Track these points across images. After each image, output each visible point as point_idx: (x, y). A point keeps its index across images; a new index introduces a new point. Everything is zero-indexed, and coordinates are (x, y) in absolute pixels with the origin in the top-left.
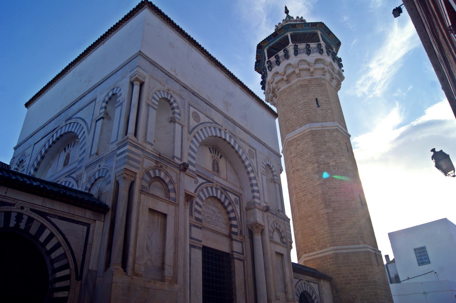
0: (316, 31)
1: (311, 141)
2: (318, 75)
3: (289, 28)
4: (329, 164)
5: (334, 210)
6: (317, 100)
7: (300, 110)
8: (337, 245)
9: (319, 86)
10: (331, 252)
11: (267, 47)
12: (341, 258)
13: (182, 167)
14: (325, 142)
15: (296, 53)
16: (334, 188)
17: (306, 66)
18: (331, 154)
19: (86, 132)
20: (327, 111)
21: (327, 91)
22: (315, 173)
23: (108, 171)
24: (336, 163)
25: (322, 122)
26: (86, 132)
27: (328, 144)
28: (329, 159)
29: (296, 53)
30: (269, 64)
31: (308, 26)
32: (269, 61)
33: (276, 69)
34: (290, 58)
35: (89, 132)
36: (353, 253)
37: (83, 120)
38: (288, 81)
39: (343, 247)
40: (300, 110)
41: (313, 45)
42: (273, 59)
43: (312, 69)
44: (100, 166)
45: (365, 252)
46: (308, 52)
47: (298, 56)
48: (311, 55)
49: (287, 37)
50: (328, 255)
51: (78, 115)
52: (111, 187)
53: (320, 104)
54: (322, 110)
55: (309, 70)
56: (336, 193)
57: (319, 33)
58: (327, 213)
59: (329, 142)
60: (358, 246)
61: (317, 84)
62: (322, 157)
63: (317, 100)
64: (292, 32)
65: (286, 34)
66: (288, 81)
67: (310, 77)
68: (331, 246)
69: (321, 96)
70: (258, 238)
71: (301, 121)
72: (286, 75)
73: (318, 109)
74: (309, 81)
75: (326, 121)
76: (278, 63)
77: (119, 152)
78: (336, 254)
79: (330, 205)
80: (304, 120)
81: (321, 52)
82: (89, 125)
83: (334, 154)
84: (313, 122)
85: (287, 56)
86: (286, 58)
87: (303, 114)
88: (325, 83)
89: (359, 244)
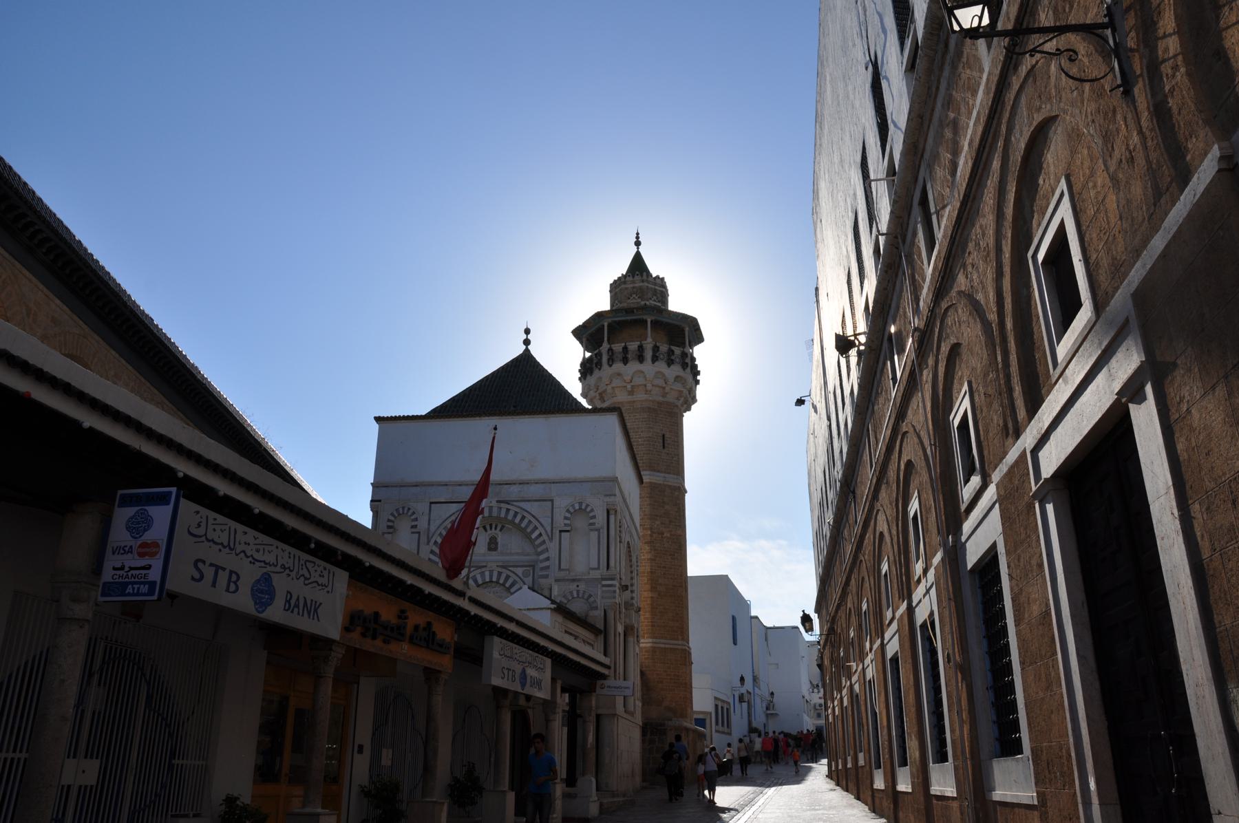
2: (671, 398)
15: (655, 359)
17: (660, 382)
19: (545, 537)
23: (590, 596)
26: (545, 537)
27: (667, 507)
29: (655, 359)
32: (610, 350)
33: (618, 366)
35: (551, 539)
38: (631, 393)
41: (677, 351)
42: (618, 347)
43: (667, 389)
46: (670, 363)
52: (599, 613)
57: (687, 329)
66: (631, 393)
67: (661, 399)
70: (631, 639)
74: (660, 403)
81: (684, 366)
82: (549, 529)
85: (641, 359)
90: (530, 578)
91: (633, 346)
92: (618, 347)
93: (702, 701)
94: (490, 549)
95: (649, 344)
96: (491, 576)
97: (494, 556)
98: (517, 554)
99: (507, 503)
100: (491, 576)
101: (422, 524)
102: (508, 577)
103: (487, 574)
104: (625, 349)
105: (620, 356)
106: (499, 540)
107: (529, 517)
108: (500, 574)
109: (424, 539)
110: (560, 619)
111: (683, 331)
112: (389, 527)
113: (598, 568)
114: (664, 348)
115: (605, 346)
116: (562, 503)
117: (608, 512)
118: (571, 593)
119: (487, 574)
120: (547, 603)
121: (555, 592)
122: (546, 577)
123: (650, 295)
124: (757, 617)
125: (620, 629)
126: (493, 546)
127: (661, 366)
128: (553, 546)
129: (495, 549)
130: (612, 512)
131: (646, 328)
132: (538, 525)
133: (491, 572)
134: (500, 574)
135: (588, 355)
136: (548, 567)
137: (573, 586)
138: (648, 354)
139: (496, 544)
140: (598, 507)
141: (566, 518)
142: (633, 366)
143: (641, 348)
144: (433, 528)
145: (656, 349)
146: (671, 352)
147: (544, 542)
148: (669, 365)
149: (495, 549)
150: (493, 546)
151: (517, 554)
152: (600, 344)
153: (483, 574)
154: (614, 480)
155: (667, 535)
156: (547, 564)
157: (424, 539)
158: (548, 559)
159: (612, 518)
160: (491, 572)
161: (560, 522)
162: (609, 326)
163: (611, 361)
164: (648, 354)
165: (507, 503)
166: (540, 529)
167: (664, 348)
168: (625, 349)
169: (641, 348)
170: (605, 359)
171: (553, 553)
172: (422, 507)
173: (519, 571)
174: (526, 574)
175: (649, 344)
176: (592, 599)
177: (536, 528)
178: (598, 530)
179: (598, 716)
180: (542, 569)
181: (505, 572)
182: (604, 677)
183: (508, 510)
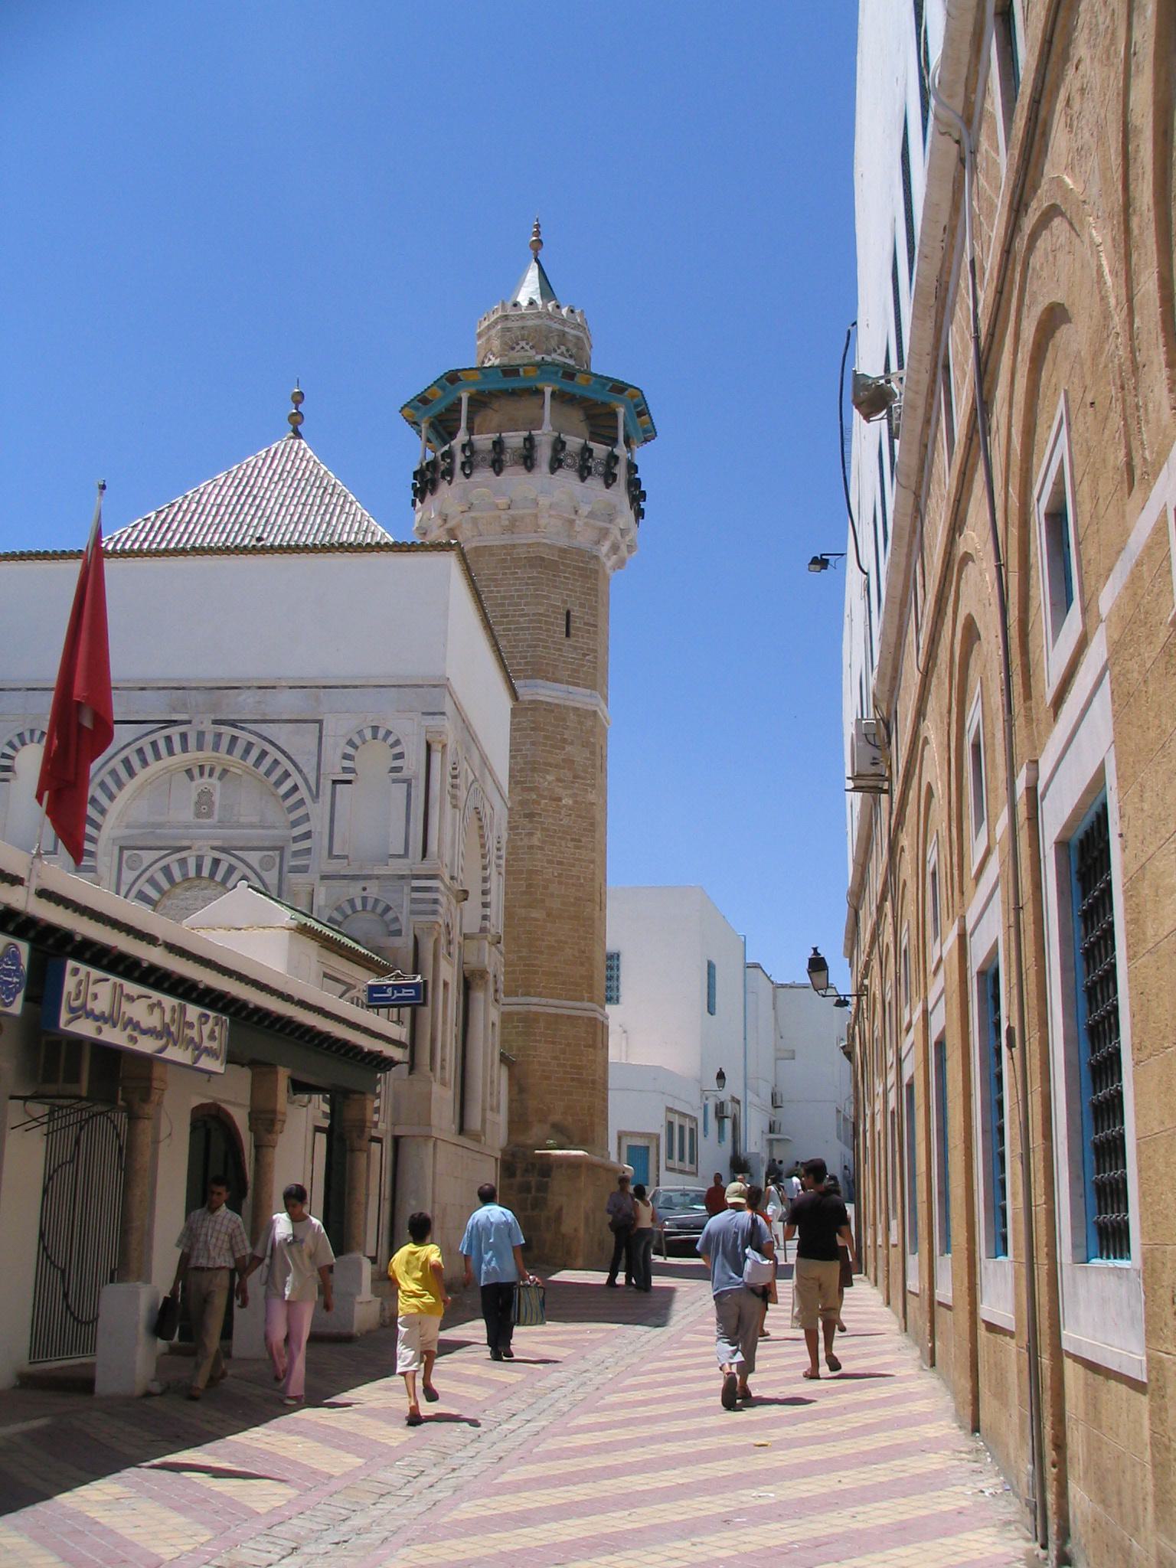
0: (615, 403)
1: (532, 729)
2: (583, 539)
3: (556, 373)
4: (560, 799)
5: (548, 915)
6: (568, 613)
7: (522, 629)
8: (540, 995)
9: (581, 575)
10: (526, 1008)
11: (473, 390)
12: (542, 1025)
13: (462, 896)
14: (564, 741)
15: (556, 464)
16: (560, 863)
18: (569, 775)
19: (303, 792)
20: (585, 655)
21: (596, 596)
22: (526, 816)
23: (388, 909)
24: (576, 802)
25: (568, 683)
26: (303, 792)
27: (568, 748)
28: (565, 788)
29: (556, 464)
30: (468, 454)
31: (604, 385)
34: (536, 470)
35: (316, 797)
36: (569, 1017)
37: (283, 752)
39: (551, 1001)
40: (522, 629)
41: (600, 450)
44: (364, 889)
45: (590, 1019)
47: (560, 472)
48: (589, 481)
49: (539, 393)
50: (518, 1013)
51: (266, 729)
52: (405, 943)
53: (572, 631)
54: (575, 648)
55: (572, 522)
56: (560, 875)
57: (621, 411)
58: (536, 920)
59: (572, 743)
60: (578, 1004)
61: (578, 568)
62: (550, 778)
63: (568, 613)
64: (557, 387)
65: (540, 385)
68: (528, 994)
69: (582, 605)
70: (478, 996)
71: (519, 664)
72: (511, 512)
73: (567, 642)
75: (577, 685)
76: (498, 466)
77: (416, 883)
78: (536, 1013)
79: (543, 901)
80: (526, 664)
83: (575, 777)
84: (548, 679)
86: (525, 463)
87: (529, 646)
88: (597, 572)
89: (581, 999)
90: (275, 871)
91: (514, 439)
92: (484, 441)
93: (630, 1114)
94: (198, 815)
95: (544, 437)
96: (199, 868)
98: (252, 826)
99: (233, 724)
100: (199, 868)
104: (498, 444)
105: (490, 457)
106: (217, 798)
107: (273, 753)
108: (216, 862)
110: (312, 947)
111: (614, 415)
113: (406, 855)
114: (574, 443)
115: (462, 437)
116: (338, 729)
117: (429, 746)
118: (351, 902)
120: (285, 916)
121: (320, 899)
122: (304, 869)
123: (554, 343)
124: (757, 966)
125: (449, 972)
127: (567, 478)
128: (318, 812)
130: (436, 747)
131: (542, 407)
132: (291, 769)
133: (200, 860)
134: (216, 862)
135: (430, 456)
136: (308, 851)
137: (354, 890)
138: (544, 454)
139: (211, 804)
140: (411, 734)
141: (346, 757)
142: (515, 479)
143: (530, 440)
145: (559, 445)
146: (587, 451)
147: (302, 802)
148: (583, 479)
149: (209, 815)
151: (252, 826)
152: (452, 435)
153: (183, 862)
154: (442, 685)
155: (567, 801)
156: (305, 844)
158: (308, 835)
159: (436, 758)
160: (200, 860)
161: (333, 766)
162: (470, 399)
163: (469, 466)
164: (544, 454)
165: (233, 724)
166: (296, 778)
167: (574, 443)
168: (498, 444)
169: (530, 440)
170: (459, 458)
171: (318, 824)
173: (253, 857)
174: (266, 864)
175: (544, 437)
176: (391, 915)
177: (287, 775)
178: (408, 782)
179: (397, 1140)
180: (296, 854)
181: (227, 861)
182: (384, 1063)
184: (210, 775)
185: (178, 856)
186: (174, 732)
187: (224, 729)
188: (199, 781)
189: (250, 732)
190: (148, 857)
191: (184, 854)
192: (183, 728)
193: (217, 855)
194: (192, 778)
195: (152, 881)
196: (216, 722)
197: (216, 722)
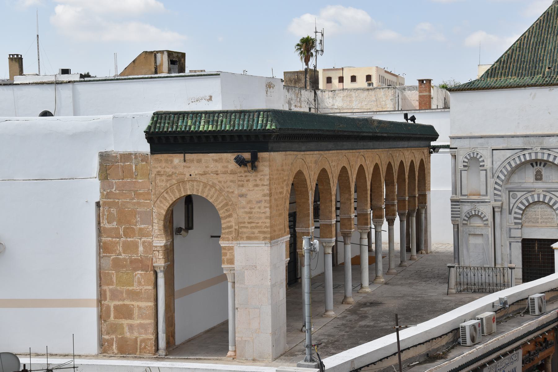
94: (537, 179)
96: (539, 197)
97: (539, 184)
99: (549, 149)
101: (488, 164)
102: (551, 199)
103: (536, 196)
106: (543, 173)
109: (489, 174)
112: (465, 166)
119: (536, 196)
126: (539, 177)
129: (541, 179)
133: (539, 195)
144: (496, 166)
149: (541, 179)
150: (539, 177)
157: (489, 174)
160: (539, 195)
165: (549, 149)
172: (485, 154)
181: (549, 195)
183: (549, 155)
184: (540, 165)
185: (530, 194)
186: (526, 152)
187: (545, 151)
188: (535, 167)
189: (555, 152)
190: (519, 194)
191: (533, 193)
192: (530, 151)
193: (545, 193)
194: (533, 166)
195: (522, 203)
196: (541, 149)
197: (541, 149)
